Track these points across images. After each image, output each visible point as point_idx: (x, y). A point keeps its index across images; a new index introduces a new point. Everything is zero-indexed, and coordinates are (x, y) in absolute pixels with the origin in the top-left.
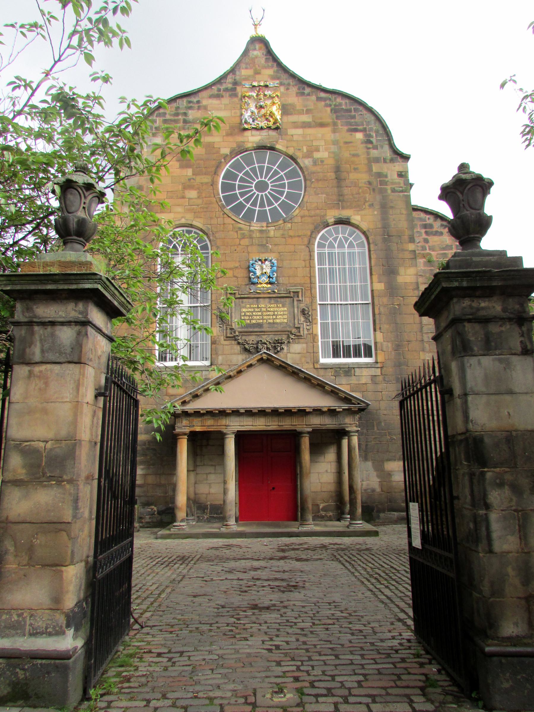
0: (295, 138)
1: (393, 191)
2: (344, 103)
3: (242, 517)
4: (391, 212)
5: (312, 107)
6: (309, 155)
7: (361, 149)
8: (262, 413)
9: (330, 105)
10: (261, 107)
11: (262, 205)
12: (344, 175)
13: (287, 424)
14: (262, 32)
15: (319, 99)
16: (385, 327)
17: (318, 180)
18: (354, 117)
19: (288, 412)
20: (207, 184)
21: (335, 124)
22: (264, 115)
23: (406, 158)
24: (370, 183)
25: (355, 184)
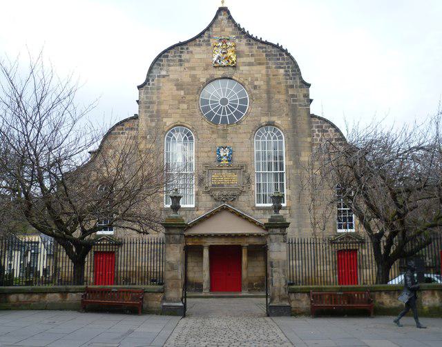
0: (244, 72)
1: (300, 105)
2: (274, 51)
3: (212, 289)
4: (298, 118)
5: (255, 53)
6: (251, 83)
7: (282, 78)
8: (223, 236)
9: (266, 52)
10: (224, 53)
11: (224, 113)
12: (272, 95)
13: (236, 242)
14: (225, 5)
15: (259, 48)
16: (292, 186)
17: (256, 99)
18: (279, 59)
19: (236, 236)
20: (192, 100)
21: (267, 64)
22: (226, 58)
23: (309, 85)
24: (287, 101)
25: (278, 101)
